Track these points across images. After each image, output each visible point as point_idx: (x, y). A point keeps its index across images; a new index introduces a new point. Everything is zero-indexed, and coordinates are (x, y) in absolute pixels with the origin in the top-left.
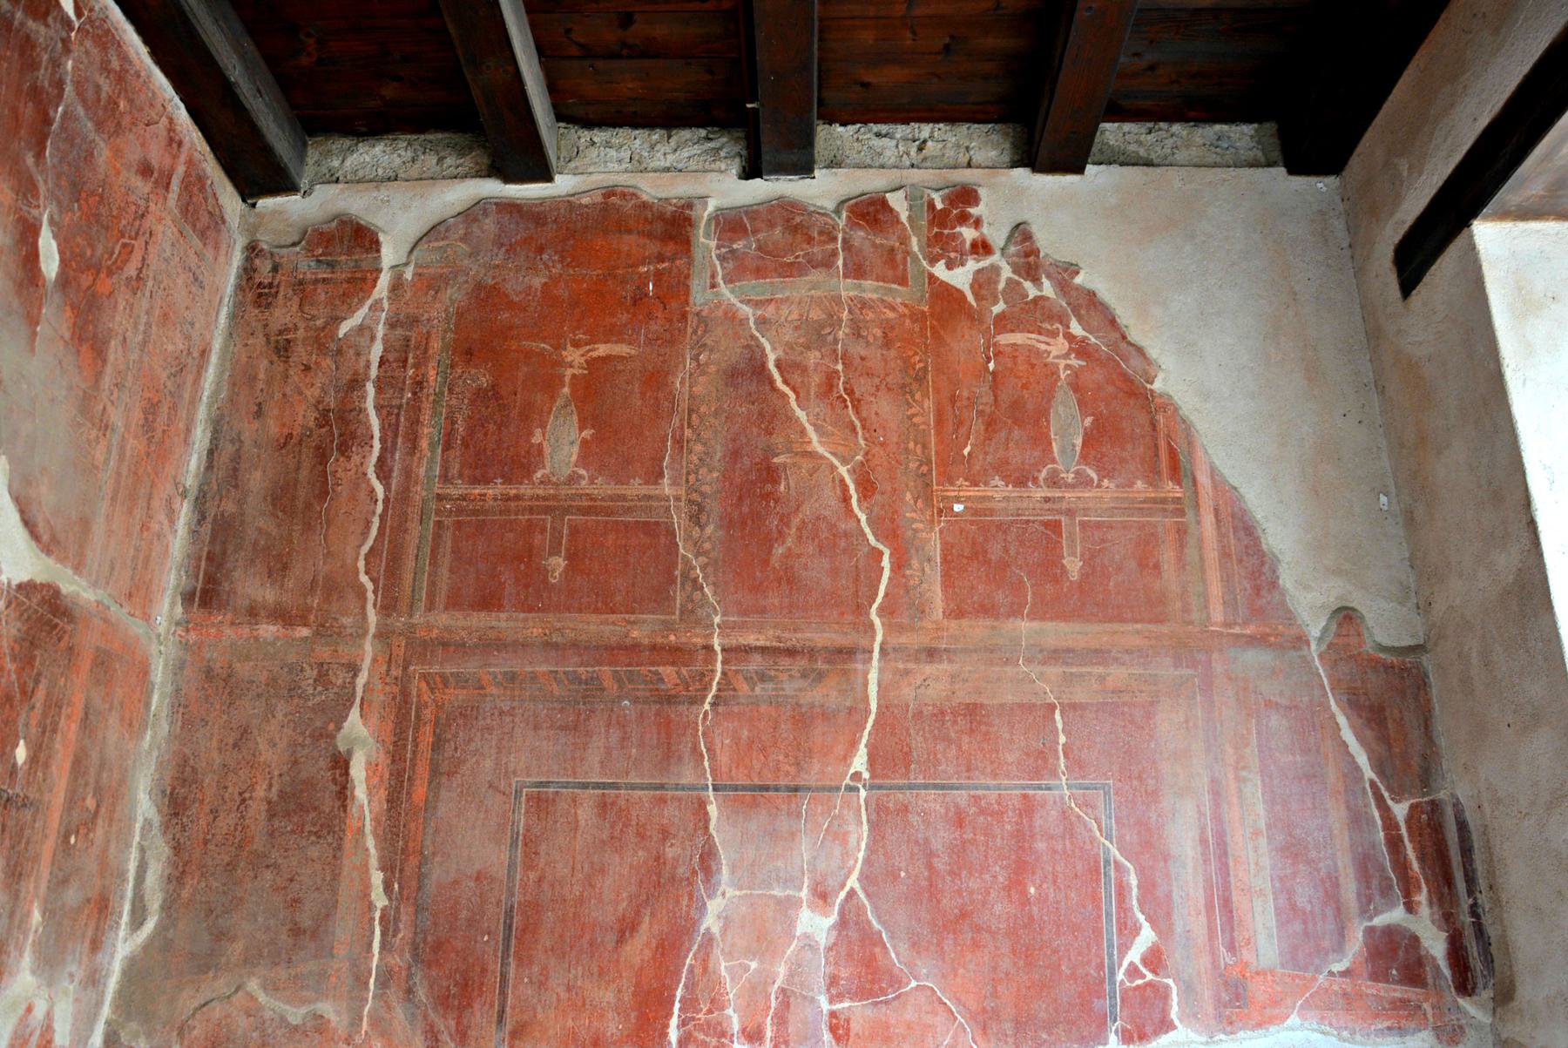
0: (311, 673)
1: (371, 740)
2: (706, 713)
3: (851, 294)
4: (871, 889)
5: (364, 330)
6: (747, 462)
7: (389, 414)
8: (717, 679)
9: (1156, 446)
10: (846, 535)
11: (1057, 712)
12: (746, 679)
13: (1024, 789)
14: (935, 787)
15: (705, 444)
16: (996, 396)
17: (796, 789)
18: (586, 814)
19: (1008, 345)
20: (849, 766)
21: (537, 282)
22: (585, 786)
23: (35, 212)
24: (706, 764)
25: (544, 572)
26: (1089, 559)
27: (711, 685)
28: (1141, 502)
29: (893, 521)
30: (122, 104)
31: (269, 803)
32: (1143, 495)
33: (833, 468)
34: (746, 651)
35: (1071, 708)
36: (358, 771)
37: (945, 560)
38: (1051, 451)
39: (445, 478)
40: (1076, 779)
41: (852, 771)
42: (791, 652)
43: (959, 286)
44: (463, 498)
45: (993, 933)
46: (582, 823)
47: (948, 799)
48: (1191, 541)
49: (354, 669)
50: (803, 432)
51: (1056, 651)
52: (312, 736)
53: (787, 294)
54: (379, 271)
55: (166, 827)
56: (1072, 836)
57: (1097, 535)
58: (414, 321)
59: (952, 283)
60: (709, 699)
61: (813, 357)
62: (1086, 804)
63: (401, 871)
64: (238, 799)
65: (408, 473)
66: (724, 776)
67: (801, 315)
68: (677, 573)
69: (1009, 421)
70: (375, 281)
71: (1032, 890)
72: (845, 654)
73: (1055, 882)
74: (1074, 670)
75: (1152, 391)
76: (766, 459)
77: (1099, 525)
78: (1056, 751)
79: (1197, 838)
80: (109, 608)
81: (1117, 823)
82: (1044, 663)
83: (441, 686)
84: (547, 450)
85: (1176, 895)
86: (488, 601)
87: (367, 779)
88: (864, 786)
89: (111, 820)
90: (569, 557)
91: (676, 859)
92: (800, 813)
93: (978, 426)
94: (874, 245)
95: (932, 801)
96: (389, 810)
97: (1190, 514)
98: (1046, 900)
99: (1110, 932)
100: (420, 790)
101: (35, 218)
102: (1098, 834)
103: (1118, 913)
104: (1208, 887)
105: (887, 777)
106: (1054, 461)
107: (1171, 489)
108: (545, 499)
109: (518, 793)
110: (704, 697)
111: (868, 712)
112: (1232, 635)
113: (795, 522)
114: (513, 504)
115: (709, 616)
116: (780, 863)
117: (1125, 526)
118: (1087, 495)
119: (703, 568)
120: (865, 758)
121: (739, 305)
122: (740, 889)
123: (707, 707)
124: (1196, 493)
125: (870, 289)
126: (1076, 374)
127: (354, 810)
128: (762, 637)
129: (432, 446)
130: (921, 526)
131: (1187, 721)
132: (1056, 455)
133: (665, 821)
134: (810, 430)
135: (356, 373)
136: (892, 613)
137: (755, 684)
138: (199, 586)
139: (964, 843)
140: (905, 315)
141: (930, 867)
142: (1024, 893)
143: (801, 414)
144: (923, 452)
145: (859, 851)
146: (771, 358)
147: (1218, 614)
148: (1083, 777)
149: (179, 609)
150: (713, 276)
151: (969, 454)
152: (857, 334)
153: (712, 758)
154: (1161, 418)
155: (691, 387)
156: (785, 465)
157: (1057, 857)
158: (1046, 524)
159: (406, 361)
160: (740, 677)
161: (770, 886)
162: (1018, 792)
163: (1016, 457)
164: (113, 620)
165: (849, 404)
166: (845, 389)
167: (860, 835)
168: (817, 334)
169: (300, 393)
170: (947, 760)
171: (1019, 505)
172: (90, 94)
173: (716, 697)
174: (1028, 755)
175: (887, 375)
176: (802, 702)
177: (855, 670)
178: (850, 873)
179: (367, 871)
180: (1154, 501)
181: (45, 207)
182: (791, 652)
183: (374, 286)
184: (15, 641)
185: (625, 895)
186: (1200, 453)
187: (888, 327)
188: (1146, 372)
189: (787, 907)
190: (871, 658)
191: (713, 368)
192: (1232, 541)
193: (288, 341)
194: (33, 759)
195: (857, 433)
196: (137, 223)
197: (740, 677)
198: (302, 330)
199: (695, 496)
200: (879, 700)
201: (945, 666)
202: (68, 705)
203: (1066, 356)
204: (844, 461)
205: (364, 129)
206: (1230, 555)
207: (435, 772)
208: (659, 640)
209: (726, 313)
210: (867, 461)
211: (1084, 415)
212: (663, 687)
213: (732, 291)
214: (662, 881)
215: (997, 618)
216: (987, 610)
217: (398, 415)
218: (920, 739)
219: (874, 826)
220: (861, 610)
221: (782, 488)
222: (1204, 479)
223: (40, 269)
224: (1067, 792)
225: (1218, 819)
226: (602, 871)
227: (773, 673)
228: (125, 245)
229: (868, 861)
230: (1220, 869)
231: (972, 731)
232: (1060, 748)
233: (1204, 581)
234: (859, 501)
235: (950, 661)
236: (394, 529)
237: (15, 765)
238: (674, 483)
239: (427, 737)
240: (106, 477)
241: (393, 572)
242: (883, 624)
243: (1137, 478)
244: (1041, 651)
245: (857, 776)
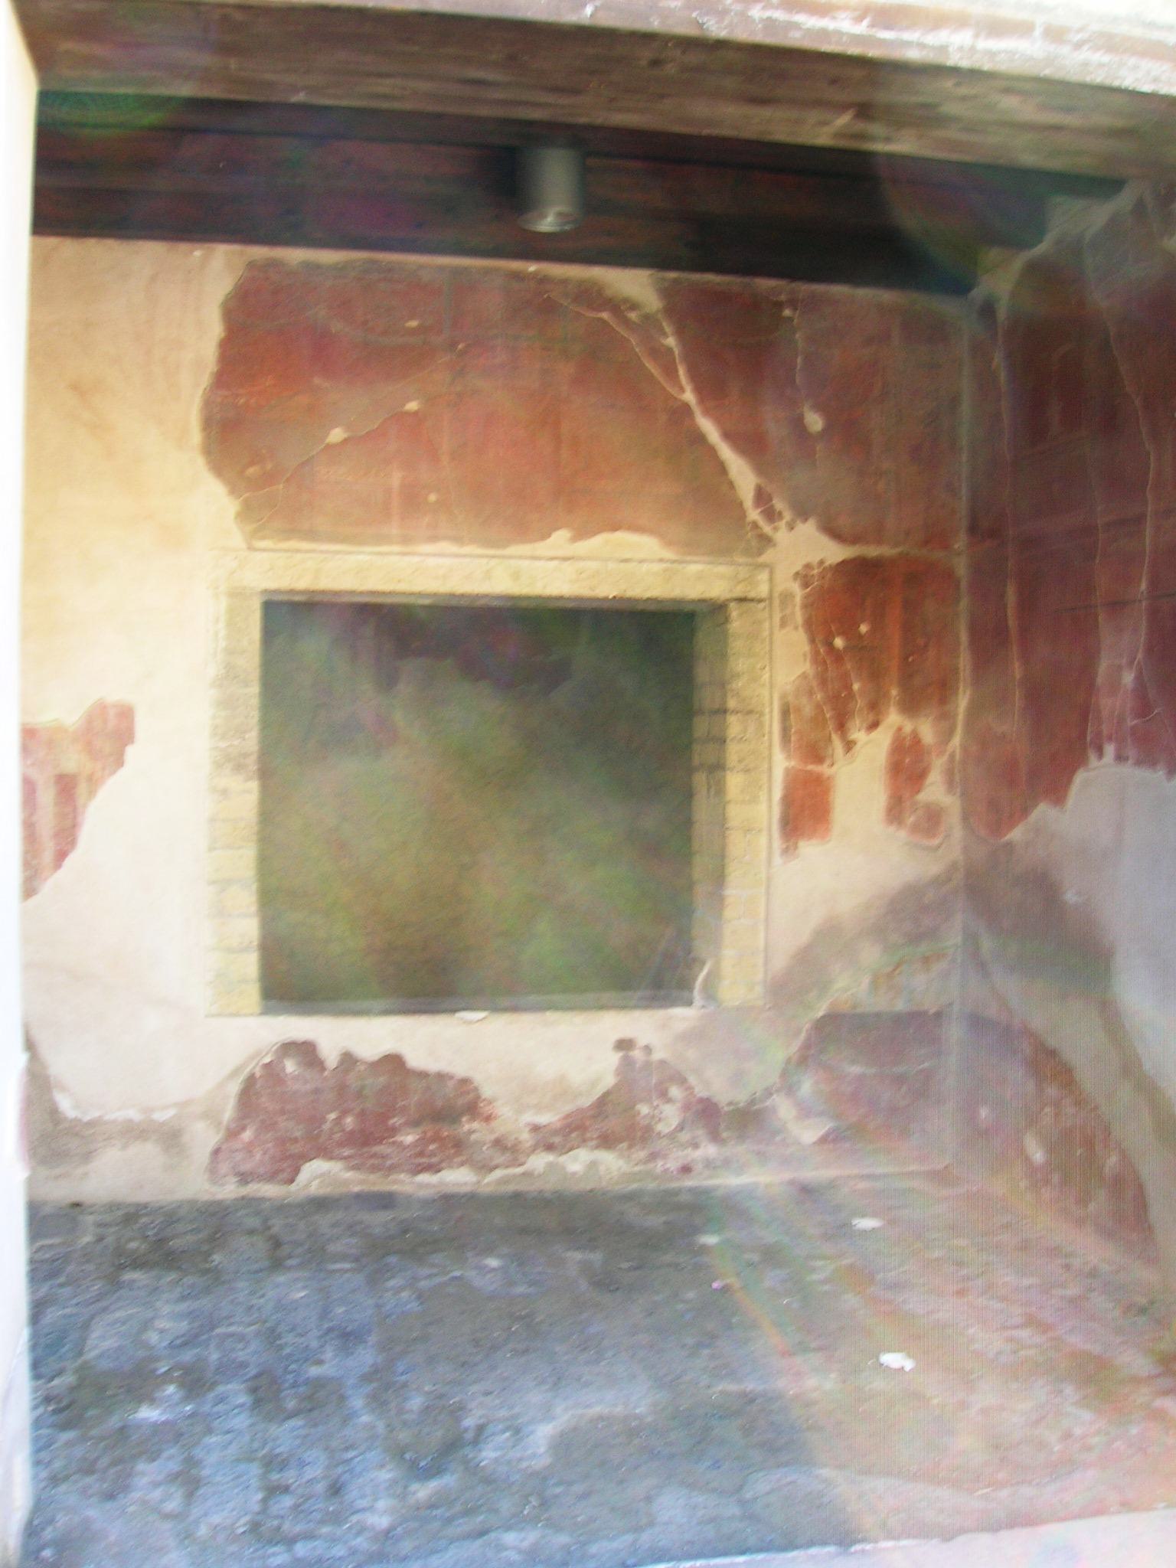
189: (1120, 668)
194: (873, 630)
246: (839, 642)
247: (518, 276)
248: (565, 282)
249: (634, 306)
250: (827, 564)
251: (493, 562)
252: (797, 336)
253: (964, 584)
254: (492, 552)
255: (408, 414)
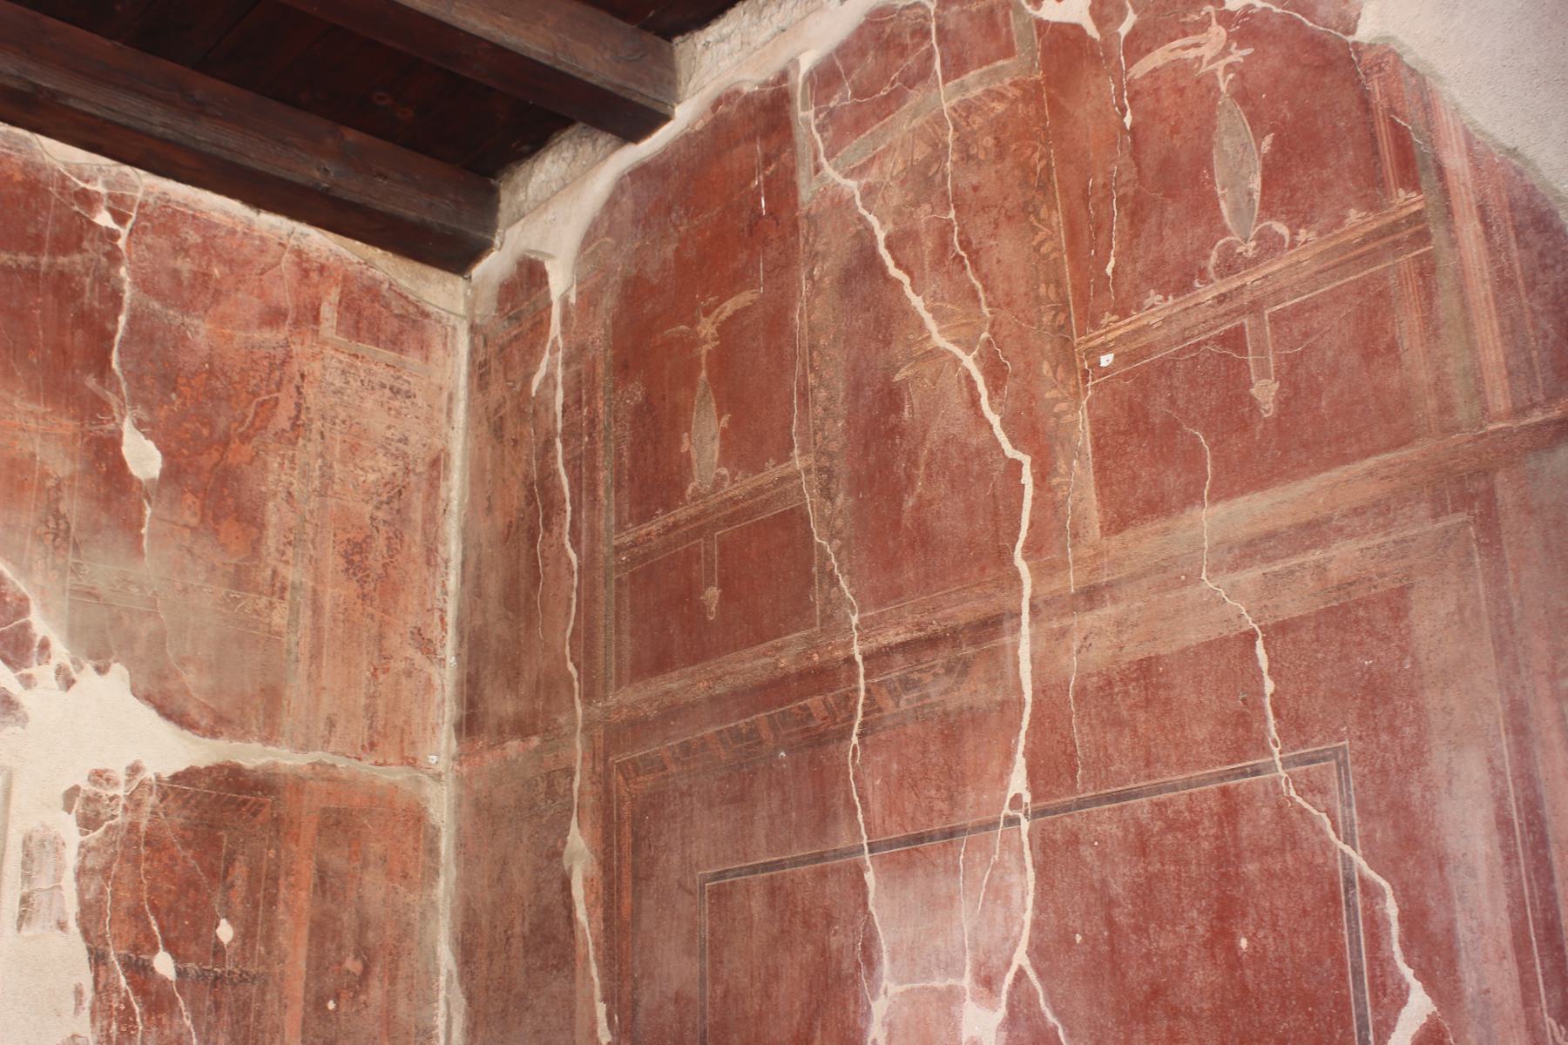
0: (542, 787)
1: (587, 852)
2: (855, 749)
3: (954, 101)
4: (1044, 965)
5: (549, 378)
6: (868, 392)
7: (574, 467)
8: (861, 700)
9: (1373, 138)
10: (979, 453)
11: (1259, 643)
12: (890, 692)
13: (1222, 779)
14: (1110, 798)
15: (827, 388)
16: (1138, 165)
17: (951, 833)
18: (758, 905)
19: (1144, 77)
20: (1006, 788)
21: (669, 250)
22: (754, 870)
23: (111, 426)
24: (860, 817)
25: (702, 609)
26: (1290, 375)
27: (855, 709)
28: (1360, 245)
29: (1030, 411)
30: (216, 272)
31: (524, 938)
32: (1362, 231)
33: (957, 361)
34: (887, 654)
35: (1280, 630)
36: (578, 892)
37: (1098, 447)
38: (1219, 217)
39: (620, 526)
40: (1293, 749)
41: (1010, 795)
42: (933, 642)
43: (1074, 20)
44: (634, 544)
45: (1194, 1018)
46: (756, 917)
47: (1126, 815)
48: (1445, 282)
49: (570, 772)
50: (921, 326)
51: (1250, 543)
52: (547, 857)
53: (889, 140)
54: (550, 305)
55: (461, 977)
56: (1294, 845)
57: (1298, 328)
58: (582, 349)
59: (1065, 19)
60: (856, 730)
61: (924, 214)
62: (1312, 788)
63: (619, 999)
64: (504, 938)
65: (593, 530)
66: (878, 830)
67: (905, 162)
68: (815, 569)
69: (1159, 196)
70: (549, 319)
71: (1244, 943)
72: (991, 626)
73: (1274, 925)
74: (1278, 567)
75: (1355, 44)
76: (887, 379)
77: (1298, 310)
78: (1262, 708)
79: (1493, 818)
80: (334, 766)
81: (1361, 811)
82: (1234, 568)
83: (633, 775)
84: (694, 456)
85: (1462, 931)
86: (660, 664)
87: (586, 897)
88: (1026, 814)
89: (393, 980)
90: (721, 586)
91: (840, 951)
92: (957, 867)
93: (1118, 219)
94: (972, 18)
95: (1105, 823)
96: (606, 929)
97: (1438, 233)
98: (1263, 958)
99: (1360, 1003)
100: (627, 901)
101: (111, 432)
102: (1332, 835)
103: (1371, 968)
104: (1517, 907)
105: (1050, 795)
106: (1225, 232)
107: (1405, 201)
108: (697, 518)
109: (702, 888)
110: (851, 727)
111: (1021, 703)
112: (1528, 428)
113: (924, 455)
114: (672, 535)
115: (847, 617)
116: (939, 942)
117: (1336, 297)
118: (1276, 268)
119: (837, 554)
120: (1024, 772)
121: (844, 182)
122: (901, 983)
123: (855, 740)
124: (1445, 192)
125: (974, 82)
126: (1240, 71)
127: (579, 935)
128: (901, 630)
129: (607, 491)
130: (1063, 406)
131: (1461, 609)
132: (1227, 220)
133: (827, 902)
134: (928, 318)
135: (548, 433)
136: (1039, 550)
137: (899, 697)
138: (465, 713)
139: (1149, 879)
140: (1014, 102)
141: (1110, 922)
142: (1232, 947)
143: (917, 302)
144: (1058, 294)
145: (1025, 910)
146: (881, 236)
147: (1500, 401)
148: (1304, 744)
149: (454, 742)
150: (816, 158)
151: (1114, 271)
152: (966, 157)
153: (865, 809)
154: (1375, 86)
155: (809, 317)
156: (905, 381)
157: (1276, 884)
158: (1222, 340)
159: (580, 400)
160: (884, 690)
161: (930, 977)
162: (1213, 786)
163: (1174, 246)
164: (345, 776)
165: (967, 262)
166: (961, 243)
167: (1025, 885)
168: (923, 180)
169: (513, 473)
170: (1120, 752)
171: (1185, 323)
172: (165, 283)
173: (863, 724)
174: (1224, 724)
175: (1005, 199)
176: (950, 707)
177: (1003, 647)
178: (1016, 944)
179: (593, 1005)
180: (1379, 234)
181: (123, 417)
182: (933, 642)
183: (549, 325)
184: (184, 829)
185: (798, 1004)
186: (1445, 118)
187: (998, 127)
188: (1342, 17)
189: (950, 998)
190: (1019, 624)
191: (827, 280)
192: (1515, 255)
193: (501, 418)
194: (246, 934)
195: (979, 301)
196: (277, 373)
197: (884, 690)
198: (508, 402)
199: (825, 462)
200: (1033, 682)
201: (1109, 610)
202: (287, 874)
203: (1225, 52)
204: (969, 349)
205: (526, 148)
206: (1511, 282)
207: (636, 879)
208: (806, 664)
209: (832, 200)
210: (994, 335)
211: (1259, 137)
212: (813, 725)
213: (835, 168)
214: (830, 981)
215: (1168, 513)
216: (1156, 507)
217: (580, 466)
218: (1086, 729)
219: (1042, 870)
220: (1003, 556)
221: (906, 414)
222: (1455, 161)
223: (131, 476)
224: (1282, 773)
225: (1527, 778)
226: (776, 977)
227: (916, 676)
228: (262, 404)
229: (1037, 925)
230: (1536, 870)
231: (1148, 701)
232: (1267, 701)
233: (1471, 346)
234: (990, 398)
235: (1115, 600)
236: (588, 601)
237: (218, 944)
238: (804, 452)
239: (628, 840)
240: (300, 640)
241: (590, 655)
242: (1030, 568)
243: (1349, 206)
244: (1231, 549)
245: (1016, 801)
246: (164, 964)
250: (149, 774)
252: (123, 271)
253: (446, 845)
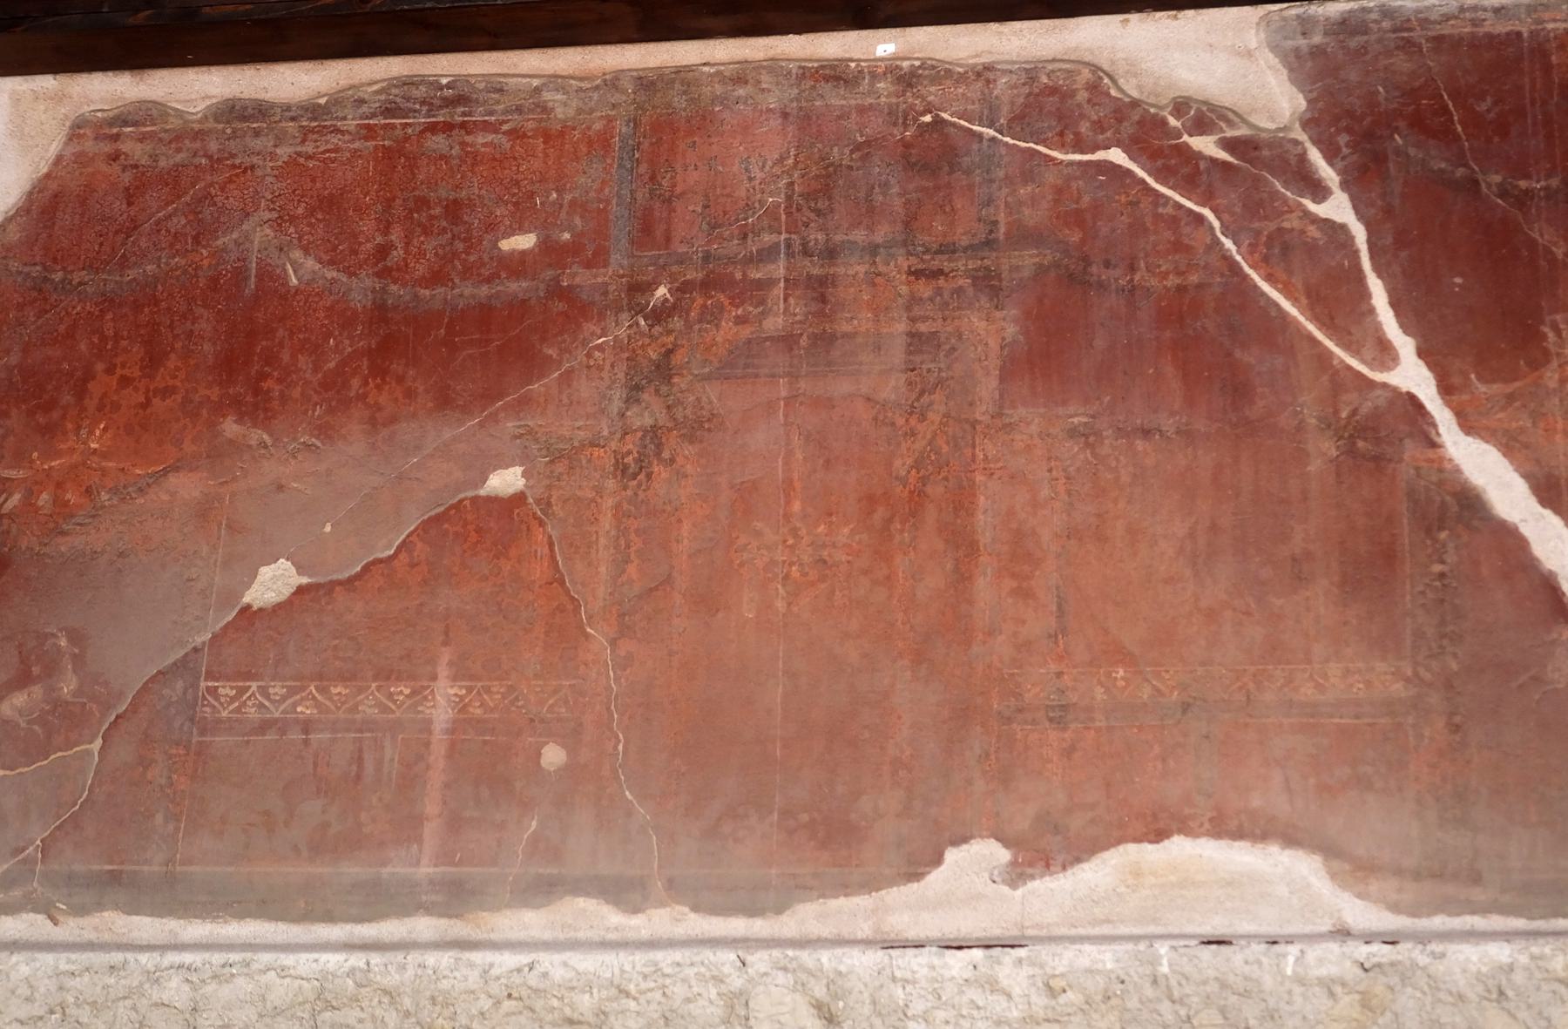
247: (835, 74)
248: (984, 73)
249: (1205, 118)
251: (760, 960)
254: (737, 926)
255: (493, 500)
